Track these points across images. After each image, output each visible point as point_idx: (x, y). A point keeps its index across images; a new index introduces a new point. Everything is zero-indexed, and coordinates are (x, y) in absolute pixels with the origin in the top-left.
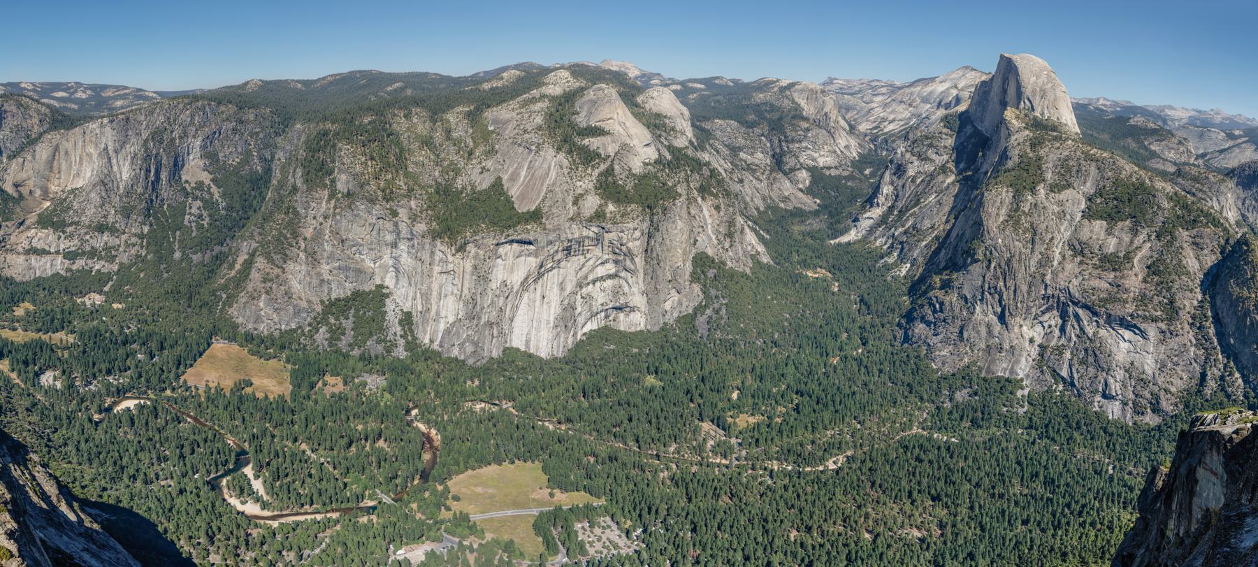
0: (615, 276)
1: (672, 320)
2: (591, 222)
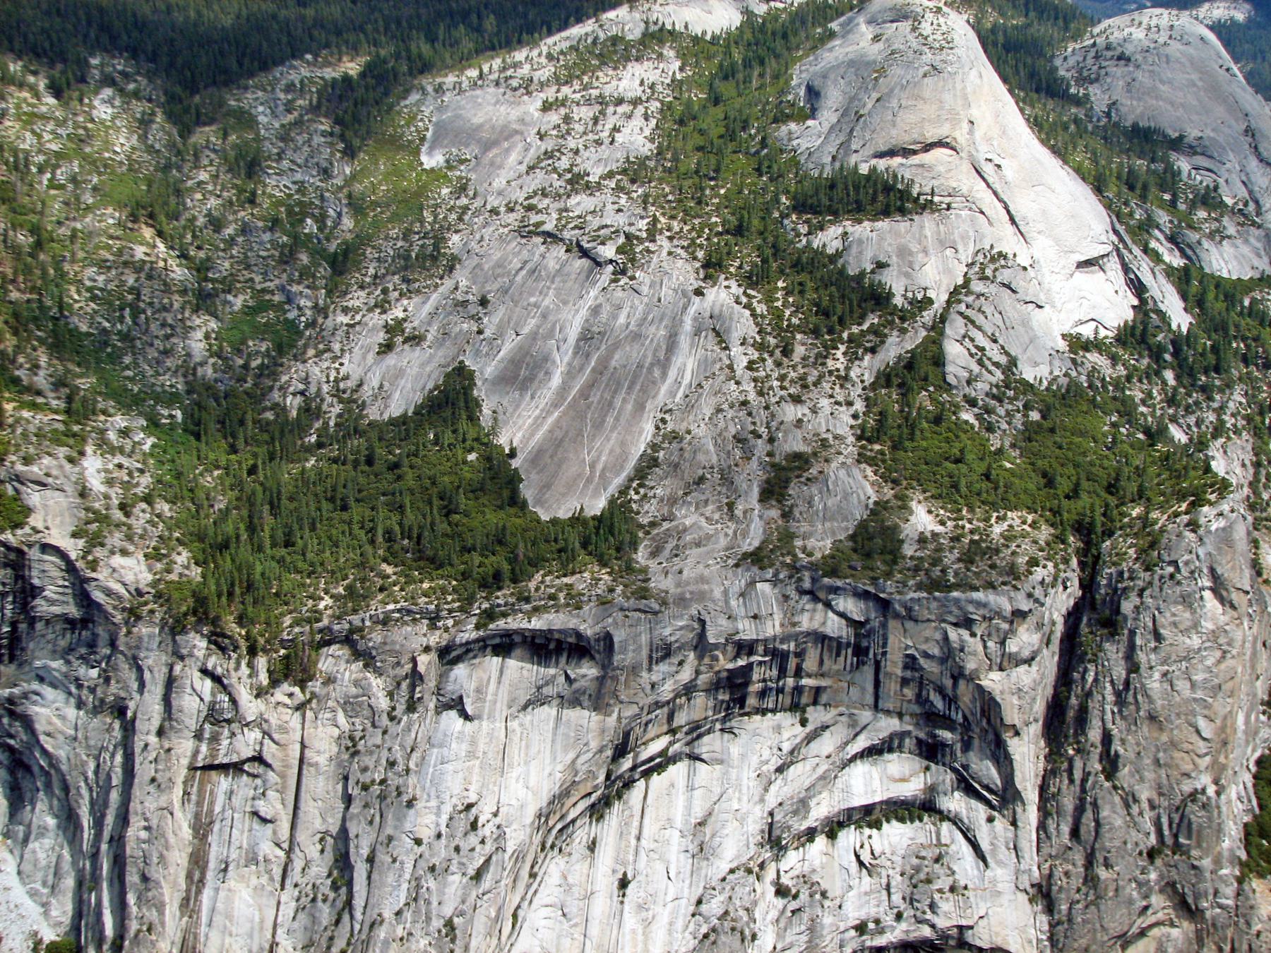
2: (834, 573)
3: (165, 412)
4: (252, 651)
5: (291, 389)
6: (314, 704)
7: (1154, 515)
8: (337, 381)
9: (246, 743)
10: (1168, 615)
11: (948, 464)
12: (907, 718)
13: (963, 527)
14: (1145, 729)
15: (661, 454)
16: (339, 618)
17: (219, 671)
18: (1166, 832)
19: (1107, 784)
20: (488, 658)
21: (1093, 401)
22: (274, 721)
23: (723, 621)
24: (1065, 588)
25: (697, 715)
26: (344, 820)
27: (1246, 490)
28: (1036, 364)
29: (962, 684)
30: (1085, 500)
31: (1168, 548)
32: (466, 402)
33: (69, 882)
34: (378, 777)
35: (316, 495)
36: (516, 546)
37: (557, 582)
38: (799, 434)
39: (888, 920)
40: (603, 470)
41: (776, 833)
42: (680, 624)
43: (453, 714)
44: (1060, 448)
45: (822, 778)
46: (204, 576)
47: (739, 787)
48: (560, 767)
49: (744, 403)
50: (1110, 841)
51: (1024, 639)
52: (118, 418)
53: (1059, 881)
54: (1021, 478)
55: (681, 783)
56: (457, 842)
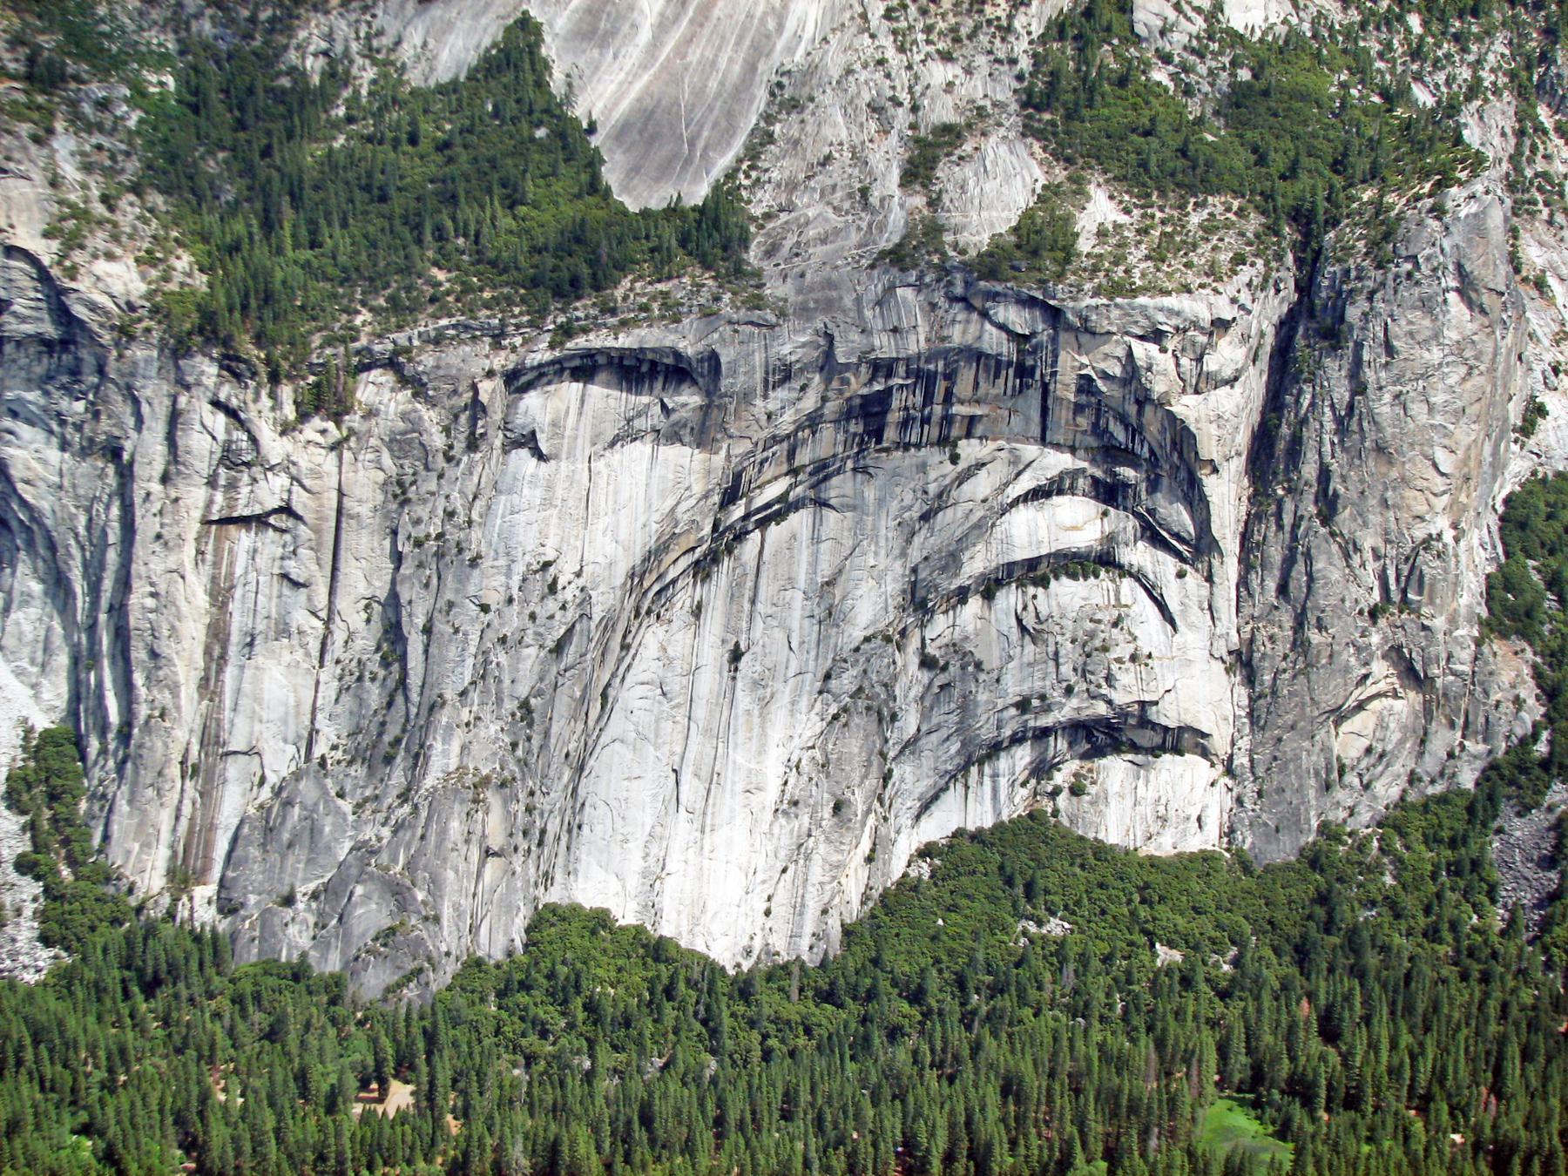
0: (1103, 560)
1: (1365, 816)
2: (992, 274)
3: (154, 78)
4: (275, 378)
5: (312, 48)
6: (353, 442)
7: (1390, 198)
8: (368, 37)
9: (270, 492)
10: (1403, 322)
11: (1134, 137)
12: (1081, 453)
13: (1153, 217)
14: (1371, 463)
15: (777, 128)
16: (380, 336)
17: (234, 402)
18: (1393, 586)
19: (1323, 530)
20: (566, 384)
21: (1317, 56)
22: (304, 464)
23: (855, 336)
24: (1278, 291)
25: (823, 451)
26: (393, 583)
27: (1505, 166)
28: (1247, 9)
29: (1148, 409)
30: (1305, 180)
31: (1406, 241)
32: (533, 63)
33: (62, 660)
34: (433, 531)
35: (347, 183)
36: (598, 245)
37: (650, 289)
38: (949, 100)
39: (1056, 695)
40: (705, 149)
41: (921, 593)
42: (803, 339)
43: (524, 453)
44: (1275, 115)
45: (977, 526)
46: (211, 285)
47: (875, 538)
48: (657, 517)
49: (881, 62)
50: (1324, 598)
51: (1226, 355)
52: (94, 86)
53: (1263, 647)
54: (1226, 153)
55: (805, 534)
56: (532, 608)
